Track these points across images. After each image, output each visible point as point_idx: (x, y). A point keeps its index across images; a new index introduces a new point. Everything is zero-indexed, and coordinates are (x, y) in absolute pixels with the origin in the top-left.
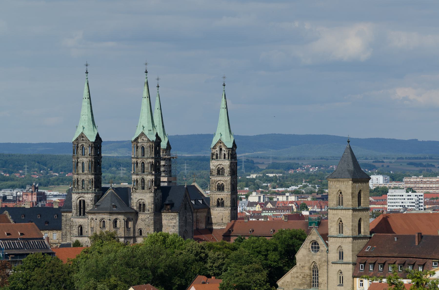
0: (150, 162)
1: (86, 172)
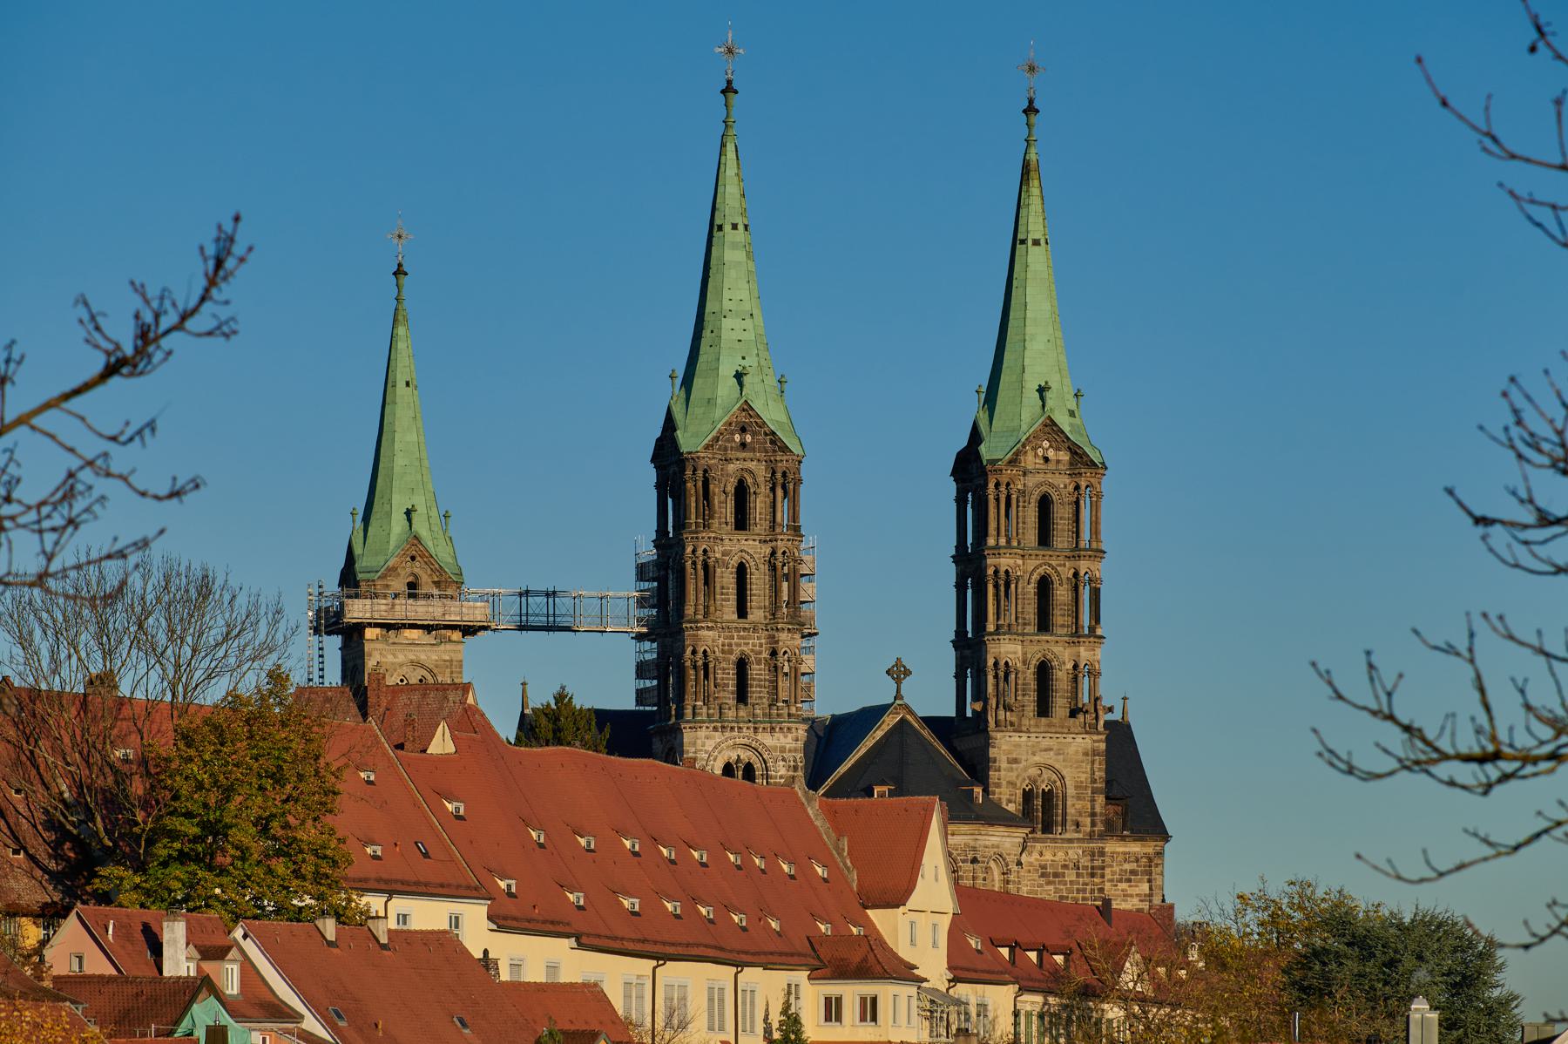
1: (757, 615)
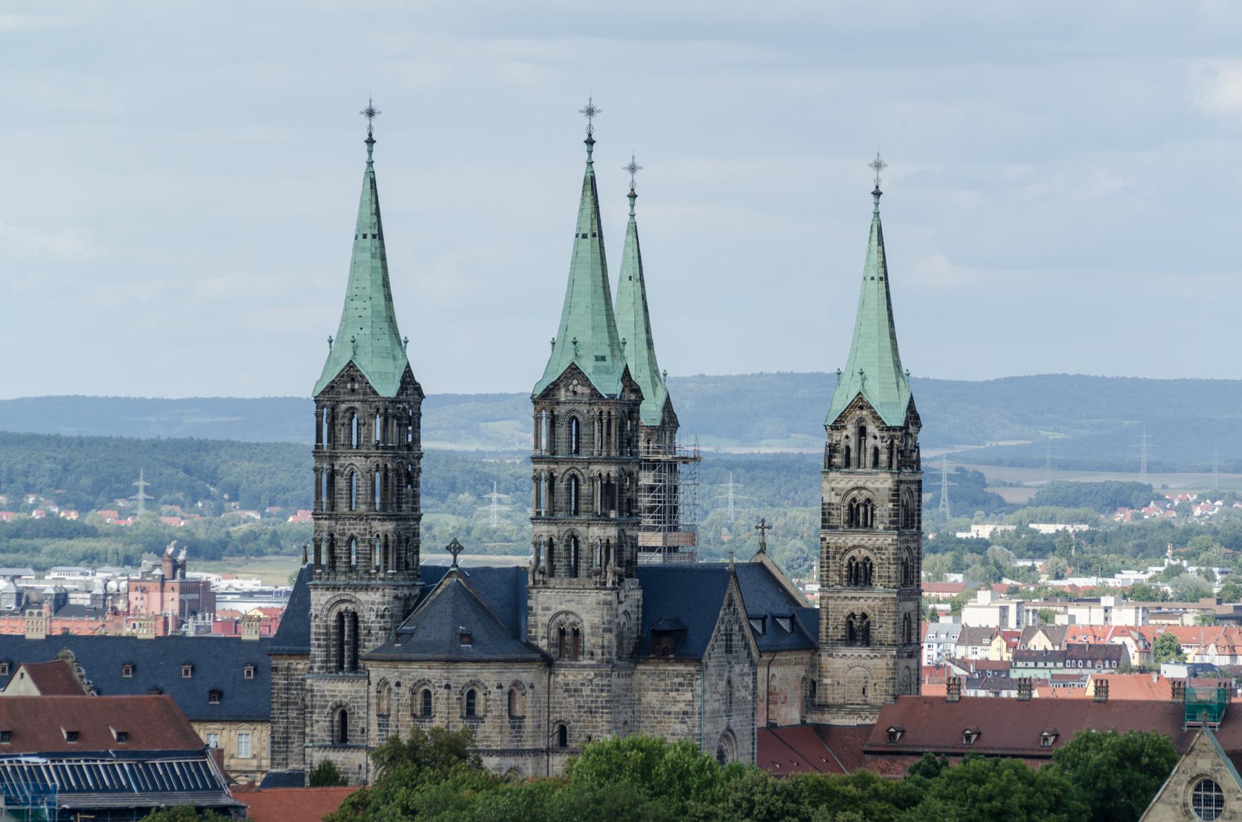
0: (600, 475)
